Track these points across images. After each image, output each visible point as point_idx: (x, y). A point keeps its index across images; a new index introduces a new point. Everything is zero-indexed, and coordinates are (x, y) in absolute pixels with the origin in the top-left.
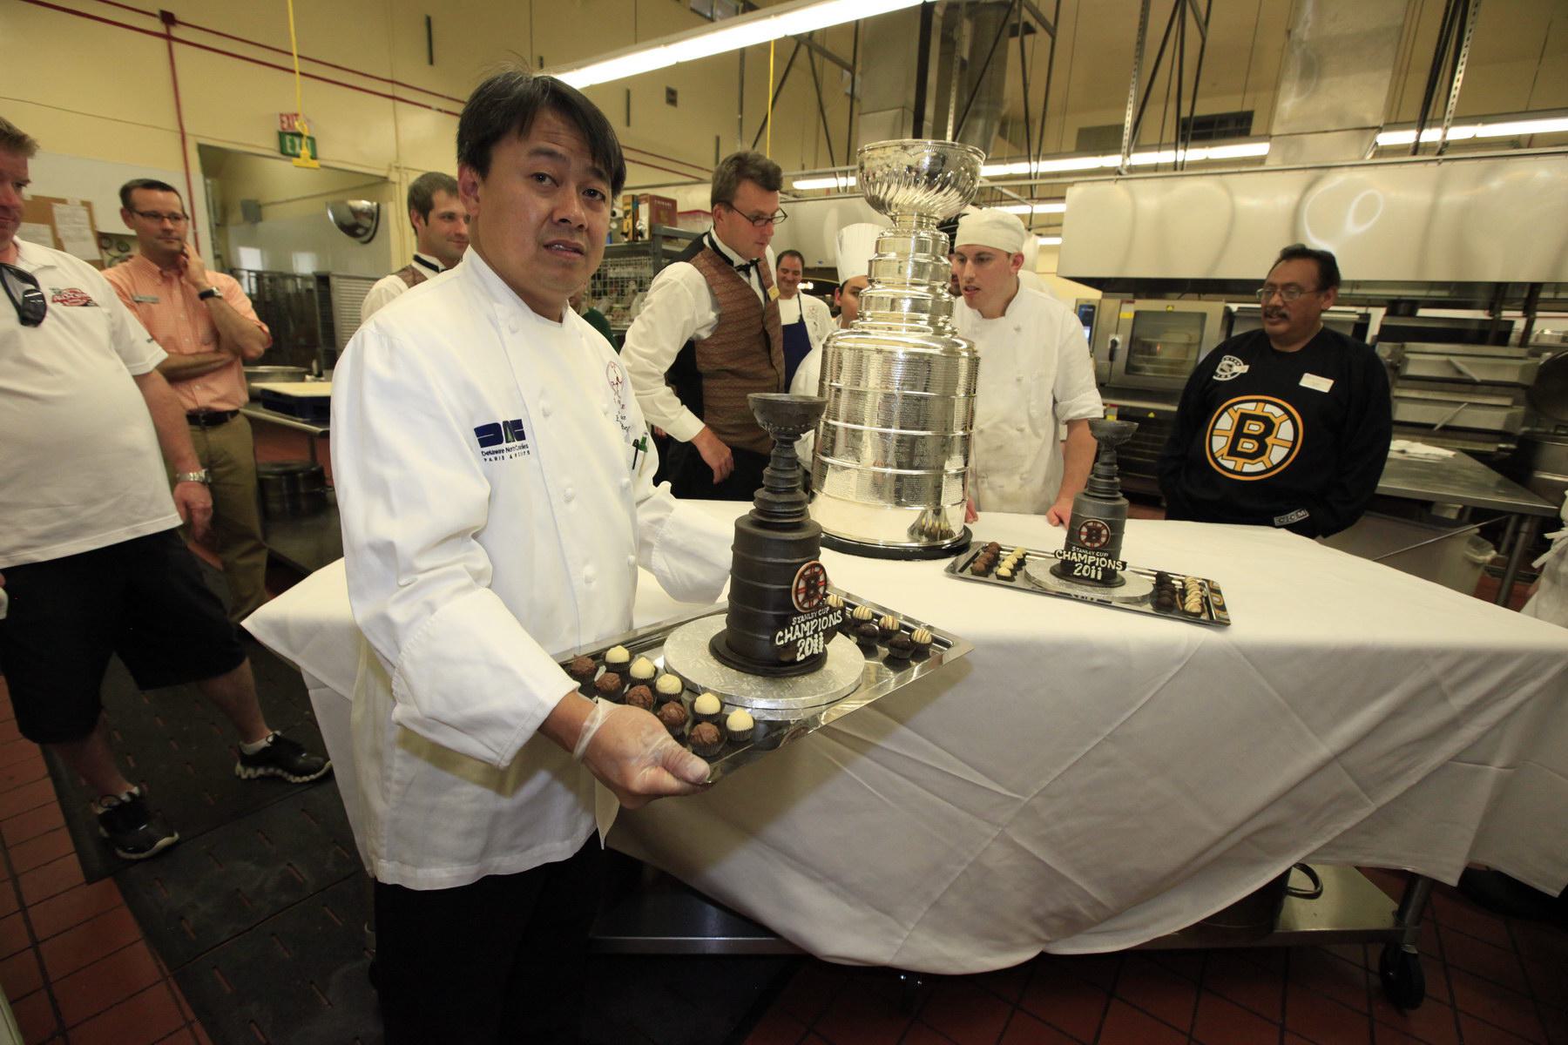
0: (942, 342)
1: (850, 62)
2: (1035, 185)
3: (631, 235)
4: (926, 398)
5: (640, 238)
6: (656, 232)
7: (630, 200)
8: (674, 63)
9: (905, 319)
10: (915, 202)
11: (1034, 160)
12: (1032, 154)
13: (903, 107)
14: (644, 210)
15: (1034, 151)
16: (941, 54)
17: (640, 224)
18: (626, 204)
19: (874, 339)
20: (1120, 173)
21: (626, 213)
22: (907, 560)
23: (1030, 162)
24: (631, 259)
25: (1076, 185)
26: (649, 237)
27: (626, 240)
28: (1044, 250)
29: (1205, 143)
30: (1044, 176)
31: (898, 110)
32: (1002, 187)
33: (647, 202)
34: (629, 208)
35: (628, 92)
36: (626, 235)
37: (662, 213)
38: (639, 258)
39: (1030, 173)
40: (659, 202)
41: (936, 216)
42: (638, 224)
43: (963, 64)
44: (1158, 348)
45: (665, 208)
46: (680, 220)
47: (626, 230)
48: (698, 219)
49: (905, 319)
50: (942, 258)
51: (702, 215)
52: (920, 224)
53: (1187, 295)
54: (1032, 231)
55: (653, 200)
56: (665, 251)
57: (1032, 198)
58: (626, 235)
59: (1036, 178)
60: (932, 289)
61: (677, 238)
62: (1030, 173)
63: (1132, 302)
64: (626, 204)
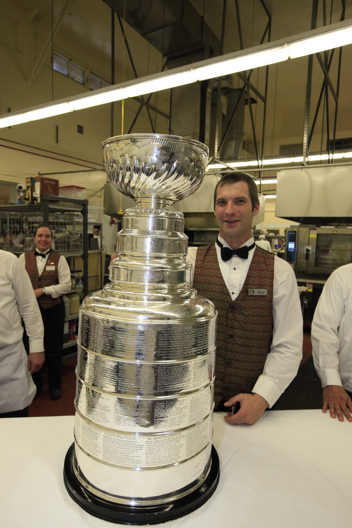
0: (176, 311)
1: (169, 115)
2: (261, 171)
3: (30, 199)
4: (162, 366)
5: (35, 202)
6: (45, 198)
7: (29, 180)
8: (72, 110)
9: (147, 288)
10: (155, 187)
11: (260, 160)
12: (258, 157)
13: (194, 134)
14: (38, 185)
15: (260, 155)
16: (212, 112)
17: (35, 194)
18: (28, 183)
19: (112, 309)
20: (303, 165)
21: (28, 187)
22: (152, 524)
23: (258, 160)
24: (31, 213)
25: (281, 171)
26: (41, 201)
27: (28, 202)
28: (268, 200)
29: (339, 151)
30: (265, 167)
31: (191, 136)
32: (245, 172)
33: (39, 182)
34: (29, 184)
35: (57, 127)
36: (28, 199)
37: (49, 187)
38: (36, 213)
39: (258, 165)
40: (47, 181)
41: (171, 198)
42: (34, 193)
43: (224, 116)
44: (330, 251)
45: (51, 184)
46: (60, 191)
47: (27, 197)
48: (73, 191)
49: (147, 288)
50: (179, 233)
51: (75, 188)
52: (158, 205)
53: (341, 224)
54: (261, 193)
55: (43, 181)
56: (50, 208)
57: (260, 177)
58: (28, 199)
59: (261, 168)
60: (170, 261)
61: (59, 202)
62: (258, 165)
63: (315, 229)
64: (28, 183)
